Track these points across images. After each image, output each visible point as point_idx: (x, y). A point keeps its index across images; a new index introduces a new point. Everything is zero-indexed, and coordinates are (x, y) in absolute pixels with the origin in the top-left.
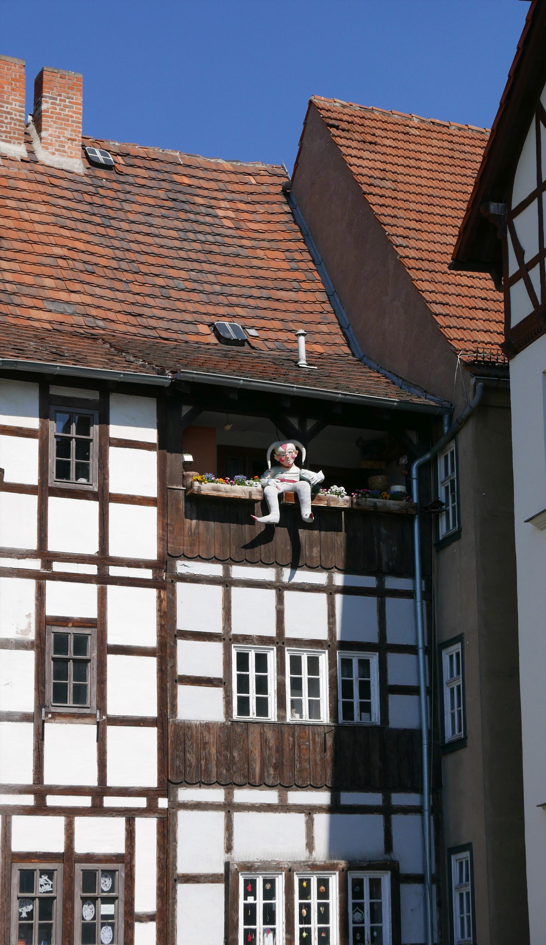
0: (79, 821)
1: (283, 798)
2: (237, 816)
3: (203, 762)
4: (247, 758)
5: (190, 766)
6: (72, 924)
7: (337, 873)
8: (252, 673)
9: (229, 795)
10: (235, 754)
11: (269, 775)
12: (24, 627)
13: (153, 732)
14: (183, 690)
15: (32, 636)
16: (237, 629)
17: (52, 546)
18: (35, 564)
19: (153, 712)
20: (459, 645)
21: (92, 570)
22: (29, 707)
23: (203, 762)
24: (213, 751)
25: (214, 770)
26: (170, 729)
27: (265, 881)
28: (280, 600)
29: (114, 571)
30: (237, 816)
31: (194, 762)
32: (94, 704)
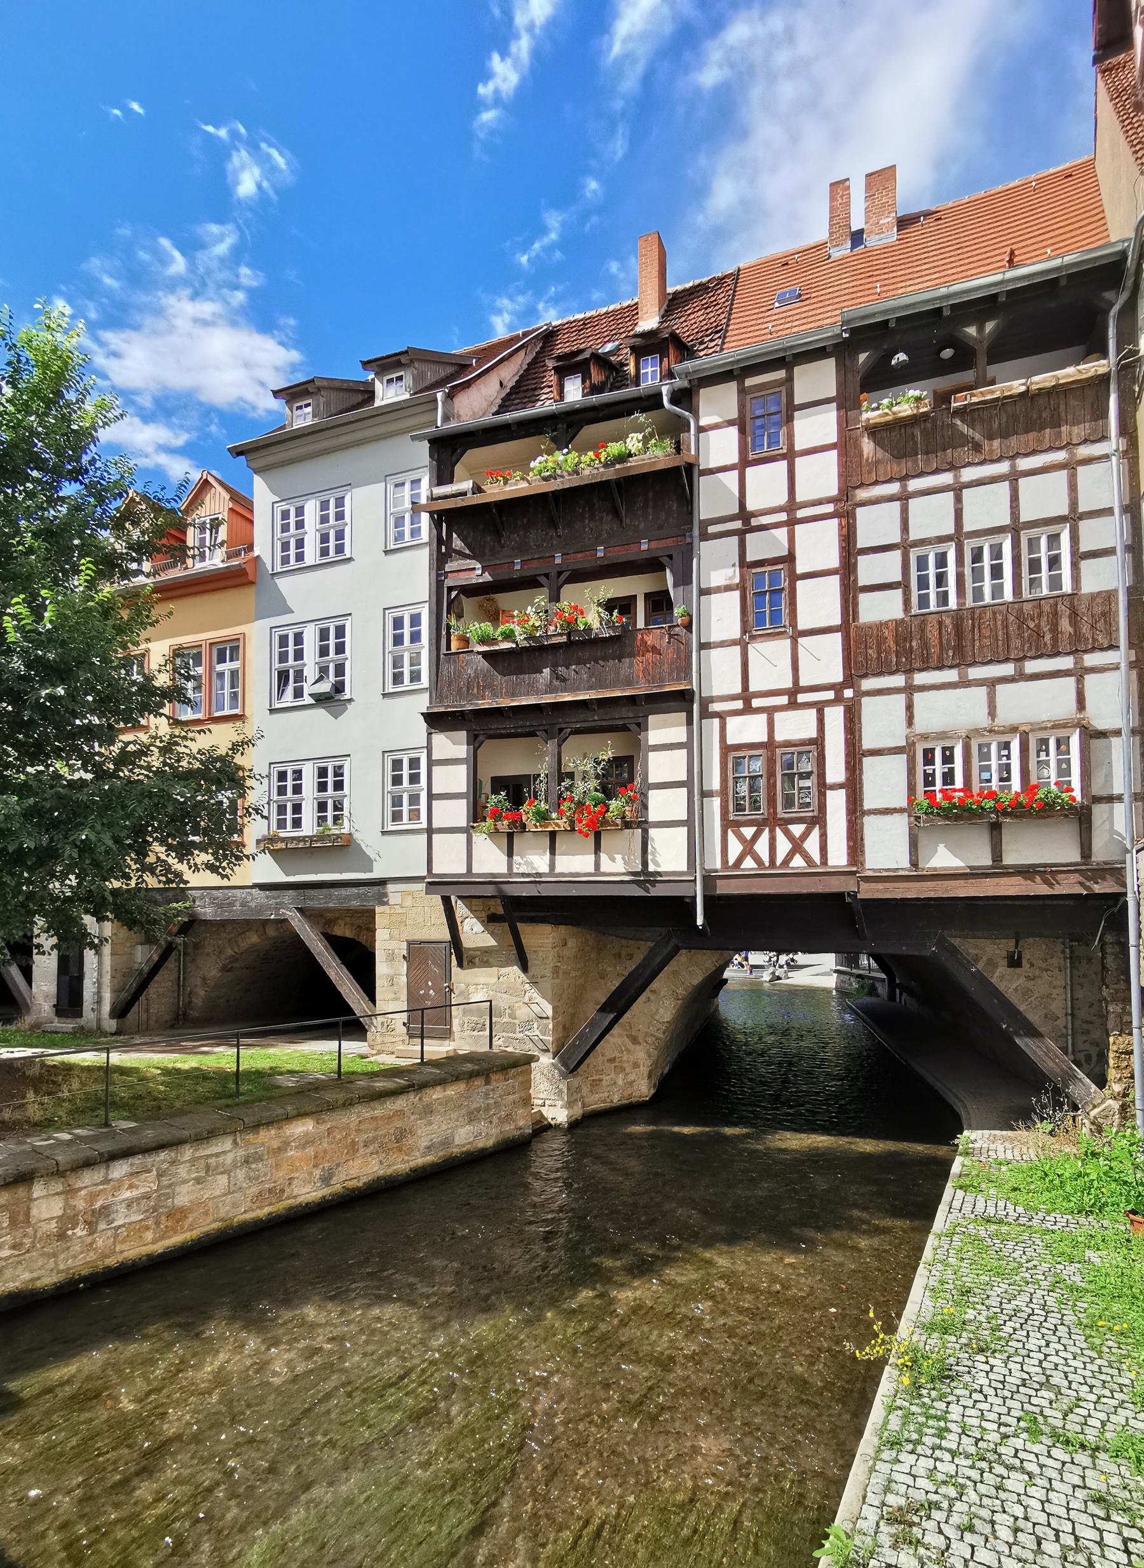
0: (778, 716)
2: (917, 696)
4: (925, 645)
6: (775, 794)
8: (932, 572)
10: (914, 644)
14: (864, 599)
15: (737, 580)
16: (914, 536)
17: (751, 506)
18: (737, 525)
19: (837, 620)
21: (783, 517)
22: (736, 633)
26: (852, 634)
27: (944, 749)
28: (958, 499)
29: (800, 514)
30: (917, 696)
32: (787, 623)
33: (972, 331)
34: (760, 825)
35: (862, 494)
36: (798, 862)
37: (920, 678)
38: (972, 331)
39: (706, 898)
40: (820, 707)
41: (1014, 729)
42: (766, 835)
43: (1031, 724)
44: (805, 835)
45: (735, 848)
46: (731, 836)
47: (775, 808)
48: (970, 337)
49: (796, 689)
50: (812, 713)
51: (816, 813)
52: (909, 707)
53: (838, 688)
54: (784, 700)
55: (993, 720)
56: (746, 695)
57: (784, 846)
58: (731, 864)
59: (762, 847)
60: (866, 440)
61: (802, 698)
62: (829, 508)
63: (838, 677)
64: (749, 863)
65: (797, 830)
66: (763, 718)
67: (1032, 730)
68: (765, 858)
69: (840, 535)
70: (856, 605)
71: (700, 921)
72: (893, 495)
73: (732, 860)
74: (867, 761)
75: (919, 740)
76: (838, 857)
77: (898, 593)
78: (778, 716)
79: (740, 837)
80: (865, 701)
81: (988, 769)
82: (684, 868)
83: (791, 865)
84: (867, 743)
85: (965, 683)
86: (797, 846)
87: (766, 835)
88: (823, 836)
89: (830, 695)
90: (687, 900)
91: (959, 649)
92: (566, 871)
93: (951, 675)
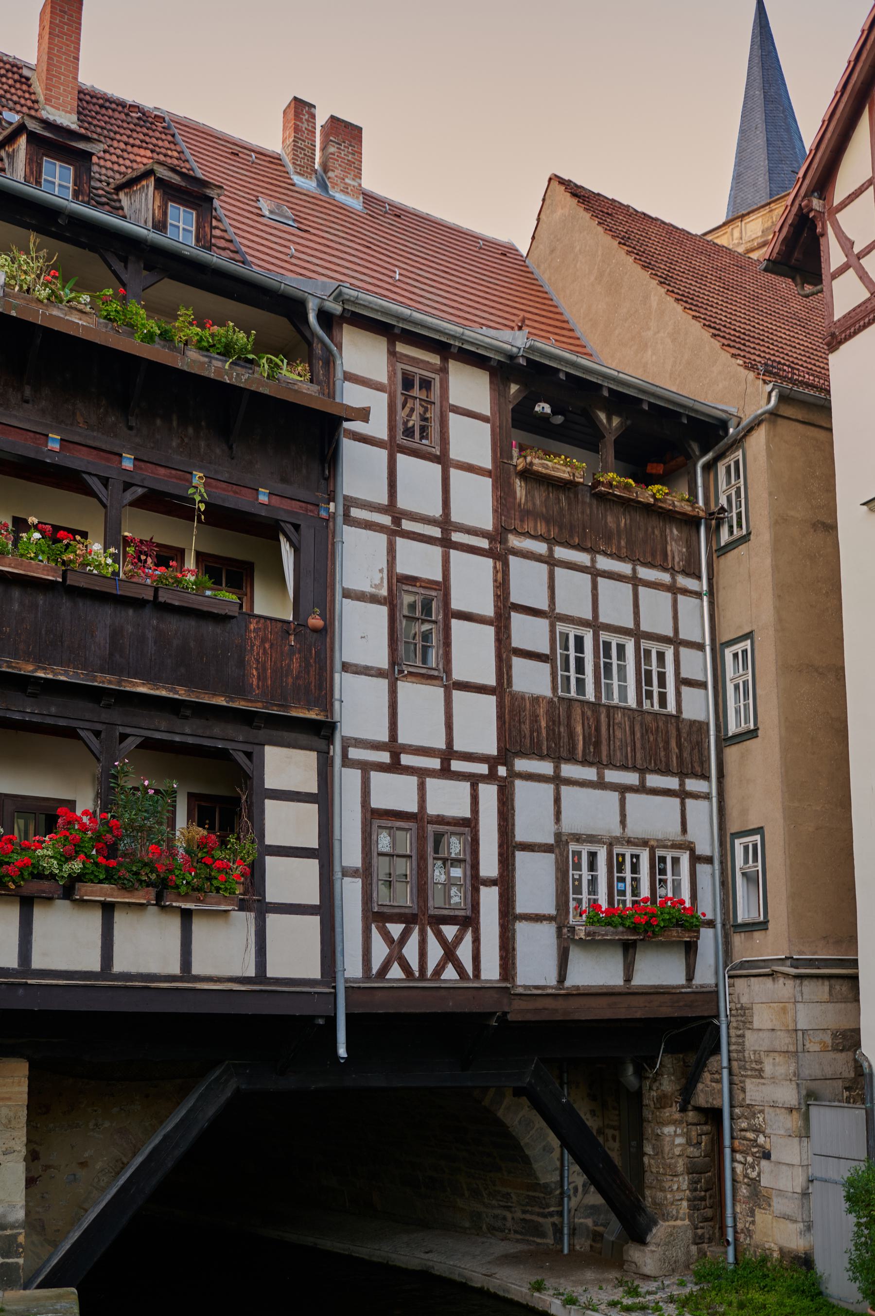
1: (601, 776)
3: (535, 734)
5: (525, 737)
7: (648, 849)
9: (557, 768)
10: (562, 730)
11: (590, 752)
12: (377, 582)
13: (491, 701)
15: (384, 592)
20: (749, 642)
23: (535, 734)
24: (543, 724)
25: (545, 743)
26: (507, 700)
31: (528, 733)
32: (441, 666)
33: (603, 416)
34: (409, 919)
35: (514, 541)
36: (450, 973)
37: (569, 770)
38: (603, 416)
39: (349, 1016)
40: (474, 780)
41: (644, 843)
42: (414, 938)
43: (658, 840)
44: (459, 939)
45: (380, 951)
46: (376, 935)
47: (426, 901)
48: (601, 421)
49: (448, 754)
50: (467, 785)
51: (469, 913)
52: (557, 800)
53: (492, 762)
54: (435, 763)
55: (624, 829)
56: (394, 747)
57: (435, 952)
58: (374, 971)
59: (411, 951)
60: (518, 481)
61: (457, 765)
62: (484, 544)
63: (492, 749)
64: (396, 972)
65: (450, 931)
66: (413, 780)
67: (658, 847)
68: (415, 965)
69: (495, 581)
70: (510, 667)
71: (342, 1052)
72: (541, 555)
73: (376, 967)
74: (520, 856)
75: (572, 840)
76: (491, 971)
77: (546, 667)
78: (430, 782)
79: (387, 936)
80: (519, 783)
81: (622, 880)
82: (317, 974)
83: (442, 978)
84: (521, 835)
85: (601, 784)
86: (450, 955)
87: (414, 938)
88: (476, 941)
89: (482, 769)
90: (321, 1022)
91: (597, 744)
92: (133, 970)
93: (589, 773)
